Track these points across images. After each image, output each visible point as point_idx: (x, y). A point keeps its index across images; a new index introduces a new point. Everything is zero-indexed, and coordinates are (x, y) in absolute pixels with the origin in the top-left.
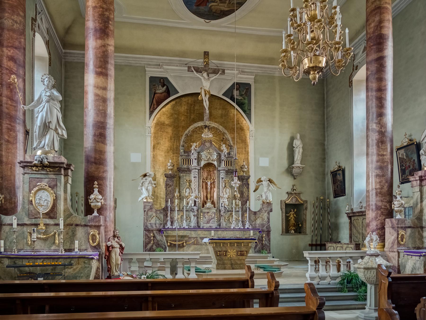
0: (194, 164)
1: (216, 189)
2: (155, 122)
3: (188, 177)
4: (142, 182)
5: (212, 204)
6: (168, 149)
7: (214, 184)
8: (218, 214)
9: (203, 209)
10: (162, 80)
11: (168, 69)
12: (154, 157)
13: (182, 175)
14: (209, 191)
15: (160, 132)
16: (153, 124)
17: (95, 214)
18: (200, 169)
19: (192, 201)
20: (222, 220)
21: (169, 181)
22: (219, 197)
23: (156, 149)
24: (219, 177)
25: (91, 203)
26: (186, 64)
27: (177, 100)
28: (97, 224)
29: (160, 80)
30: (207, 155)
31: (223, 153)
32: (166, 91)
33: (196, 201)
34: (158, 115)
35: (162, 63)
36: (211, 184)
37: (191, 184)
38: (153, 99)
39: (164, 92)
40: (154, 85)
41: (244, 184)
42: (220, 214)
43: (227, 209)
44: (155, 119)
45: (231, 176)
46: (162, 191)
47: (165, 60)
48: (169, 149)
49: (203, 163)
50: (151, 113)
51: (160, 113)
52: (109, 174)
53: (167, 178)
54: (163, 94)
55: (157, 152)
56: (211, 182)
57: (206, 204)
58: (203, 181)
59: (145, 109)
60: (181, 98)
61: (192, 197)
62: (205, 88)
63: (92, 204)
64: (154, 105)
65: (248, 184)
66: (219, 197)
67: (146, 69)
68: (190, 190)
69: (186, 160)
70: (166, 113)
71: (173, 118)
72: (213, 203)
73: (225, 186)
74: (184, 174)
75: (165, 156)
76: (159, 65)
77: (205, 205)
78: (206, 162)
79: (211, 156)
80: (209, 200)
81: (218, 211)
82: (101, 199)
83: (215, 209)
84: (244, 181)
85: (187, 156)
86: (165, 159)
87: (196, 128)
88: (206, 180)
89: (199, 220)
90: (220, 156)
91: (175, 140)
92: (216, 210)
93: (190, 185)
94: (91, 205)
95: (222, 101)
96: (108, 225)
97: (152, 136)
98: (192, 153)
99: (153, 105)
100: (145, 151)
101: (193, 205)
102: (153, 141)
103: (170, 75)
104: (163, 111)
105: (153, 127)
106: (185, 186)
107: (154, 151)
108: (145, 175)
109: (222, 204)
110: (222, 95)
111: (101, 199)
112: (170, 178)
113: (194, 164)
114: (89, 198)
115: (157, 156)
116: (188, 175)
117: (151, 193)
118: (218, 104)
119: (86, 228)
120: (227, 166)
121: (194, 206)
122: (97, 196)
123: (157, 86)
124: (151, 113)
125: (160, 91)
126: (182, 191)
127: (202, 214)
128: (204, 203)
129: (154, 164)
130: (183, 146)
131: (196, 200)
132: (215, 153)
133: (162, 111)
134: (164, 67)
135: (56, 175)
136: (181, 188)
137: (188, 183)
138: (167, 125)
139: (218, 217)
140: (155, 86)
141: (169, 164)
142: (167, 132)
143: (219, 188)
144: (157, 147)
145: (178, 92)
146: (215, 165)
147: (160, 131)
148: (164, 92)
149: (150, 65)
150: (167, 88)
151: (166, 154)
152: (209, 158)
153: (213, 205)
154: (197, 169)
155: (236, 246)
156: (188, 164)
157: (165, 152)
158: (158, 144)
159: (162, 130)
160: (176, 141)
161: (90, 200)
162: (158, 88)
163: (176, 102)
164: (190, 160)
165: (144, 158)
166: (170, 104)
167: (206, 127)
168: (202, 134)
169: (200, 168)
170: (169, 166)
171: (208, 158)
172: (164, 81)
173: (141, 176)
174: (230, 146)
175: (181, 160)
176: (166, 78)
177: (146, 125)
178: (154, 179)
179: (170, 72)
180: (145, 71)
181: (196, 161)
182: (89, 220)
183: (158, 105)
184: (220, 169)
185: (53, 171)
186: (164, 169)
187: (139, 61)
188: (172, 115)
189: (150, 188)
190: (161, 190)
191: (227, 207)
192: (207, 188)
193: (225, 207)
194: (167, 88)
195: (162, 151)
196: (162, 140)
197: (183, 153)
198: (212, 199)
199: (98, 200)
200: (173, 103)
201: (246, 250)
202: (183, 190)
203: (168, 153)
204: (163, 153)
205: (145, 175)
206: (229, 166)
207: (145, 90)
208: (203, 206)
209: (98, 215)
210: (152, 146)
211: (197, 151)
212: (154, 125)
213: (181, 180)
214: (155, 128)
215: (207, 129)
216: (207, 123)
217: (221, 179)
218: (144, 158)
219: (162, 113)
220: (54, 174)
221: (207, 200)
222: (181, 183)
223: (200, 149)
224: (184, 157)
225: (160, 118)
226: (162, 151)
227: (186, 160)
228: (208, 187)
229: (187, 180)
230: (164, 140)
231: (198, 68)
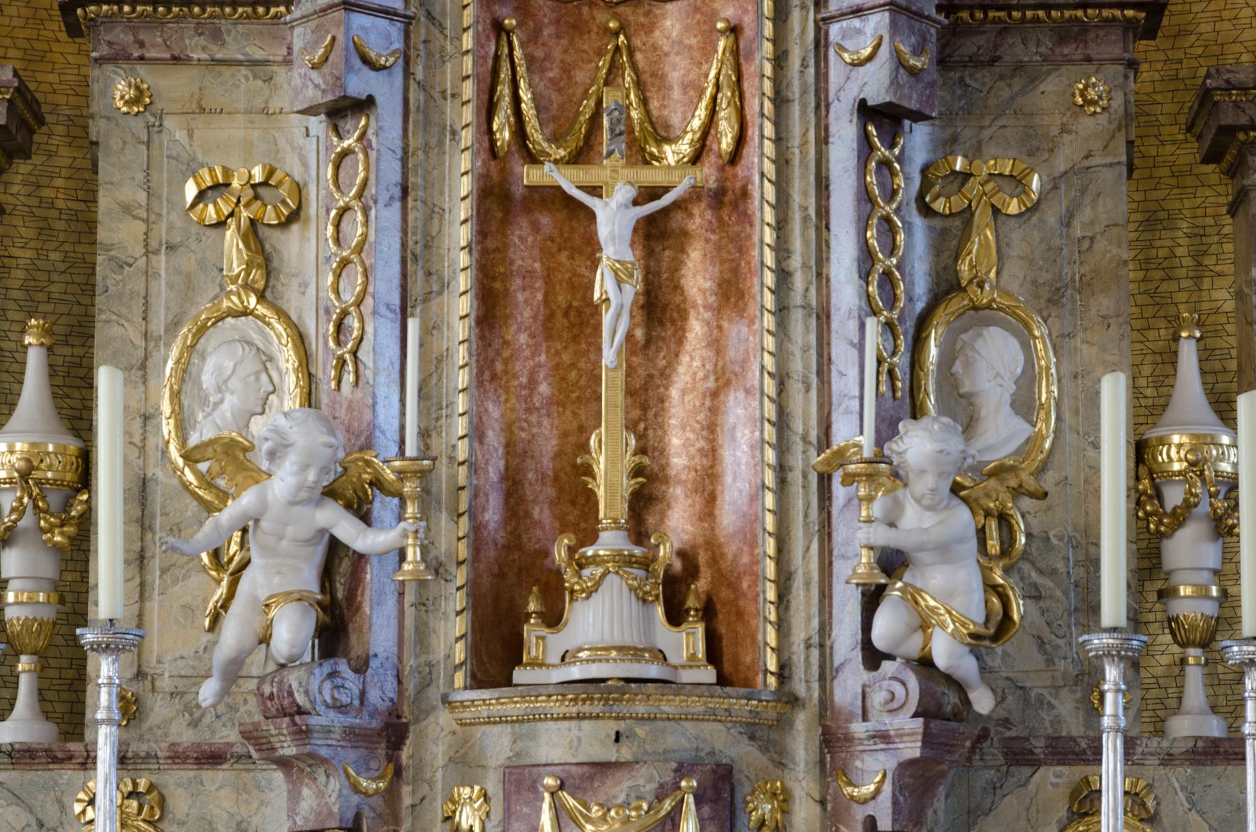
3: (234, 130)
5: (675, 617)
9: (487, 700)
33: (360, 559)
43: (983, 702)
56: (649, 194)
57: (553, 619)
68: (266, 360)
77: (532, 631)
80: (610, 541)
83: (736, 703)
116: (244, 85)
131: (348, 530)
137: (231, 238)
191: (967, 667)
193: (925, 663)
221: (591, 537)
228: (604, 284)
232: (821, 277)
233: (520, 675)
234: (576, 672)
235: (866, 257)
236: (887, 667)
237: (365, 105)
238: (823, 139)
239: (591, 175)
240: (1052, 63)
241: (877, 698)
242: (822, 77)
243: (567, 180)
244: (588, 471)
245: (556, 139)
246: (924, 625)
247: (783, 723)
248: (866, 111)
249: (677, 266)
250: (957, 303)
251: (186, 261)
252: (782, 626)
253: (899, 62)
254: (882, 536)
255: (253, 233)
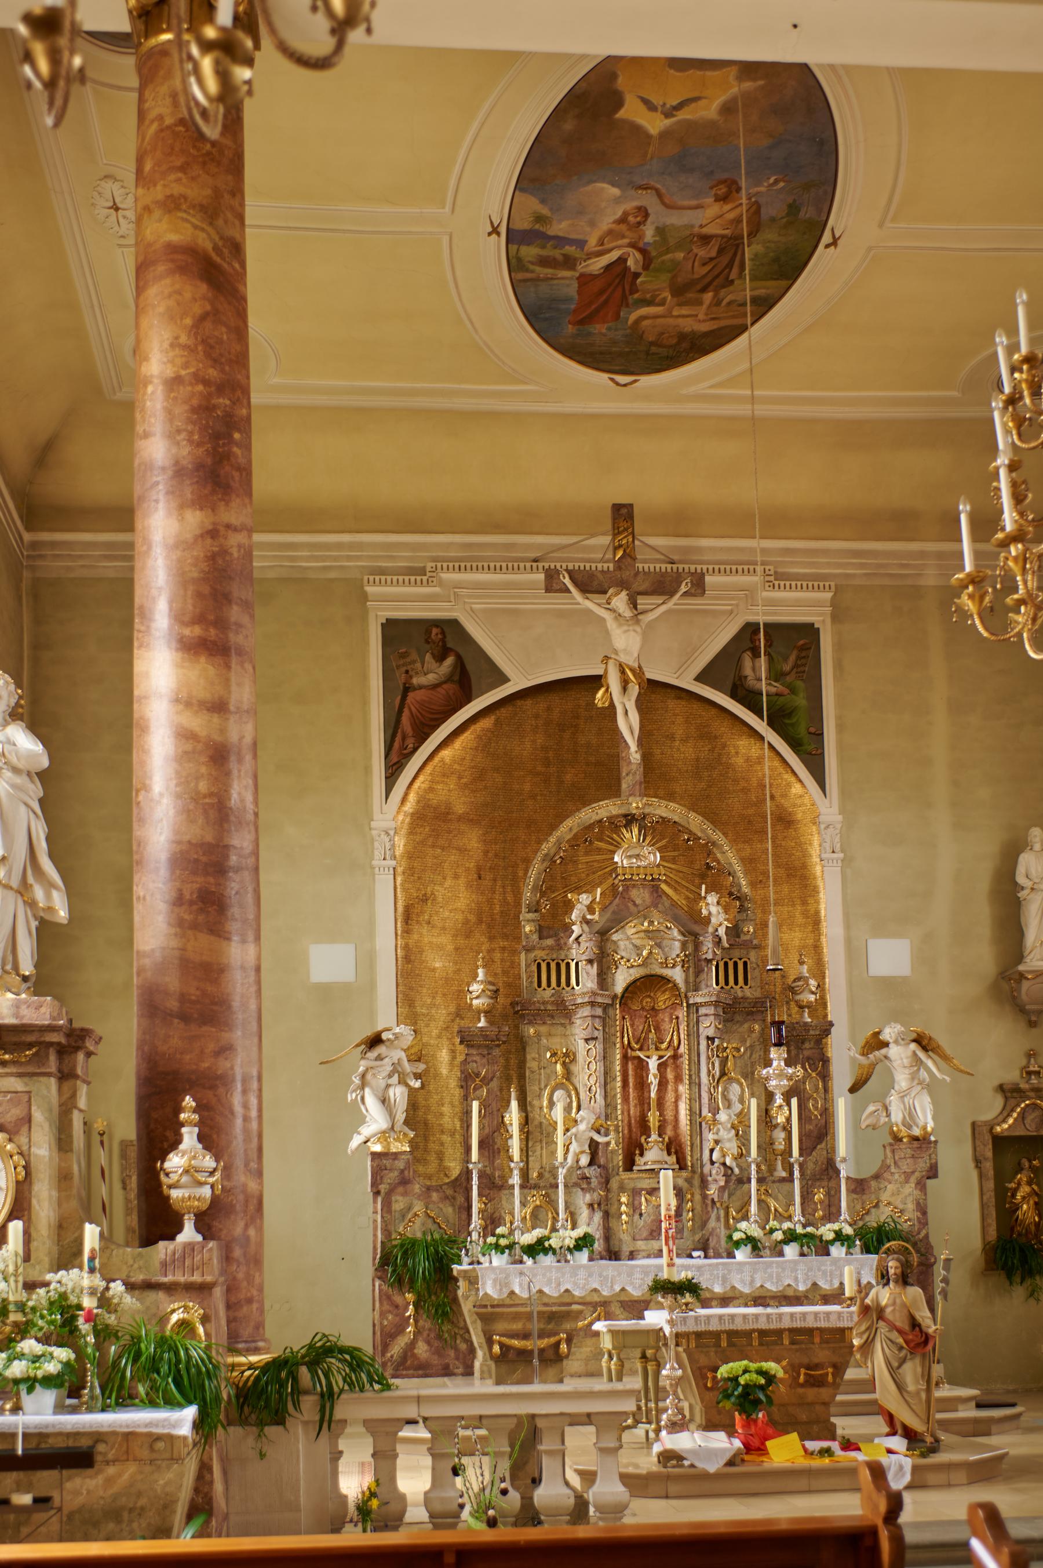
0: (586, 981)
1: (683, 1089)
2: (409, 807)
4: (361, 1069)
5: (669, 1154)
6: (466, 922)
7: (677, 1068)
8: (698, 1197)
10: (435, 631)
11: (459, 585)
12: (407, 959)
13: (532, 1031)
14: (653, 1095)
15: (430, 851)
16: (401, 817)
17: (188, 1234)
18: (612, 1005)
19: (581, 1145)
20: (712, 1223)
21: (477, 1058)
22: (697, 1125)
23: (418, 922)
24: (693, 1034)
25: (170, 1187)
26: (535, 560)
27: (503, 712)
28: (197, 1278)
29: (428, 632)
30: (638, 942)
31: (711, 929)
32: (456, 678)
33: (597, 1143)
34: (421, 778)
35: (435, 560)
36: (661, 1067)
37: (575, 1069)
38: (400, 712)
39: (445, 682)
40: (403, 656)
41: (808, 1059)
42: (704, 1197)
43: (737, 1171)
44: (412, 797)
45: (746, 1026)
46: (447, 1100)
47: (448, 546)
48: (472, 918)
49: (621, 980)
50: (393, 772)
51: (429, 769)
52: (239, 1061)
53: (468, 1046)
54: (439, 689)
55: (421, 934)
56: (661, 1057)
57: (642, 1155)
58: (625, 1058)
59: (369, 757)
60: (519, 703)
61: (582, 1127)
62: (623, 658)
63: (175, 1194)
64: (404, 739)
65: (826, 1061)
66: (697, 1125)
67: (369, 589)
68: (570, 1096)
69: (548, 965)
70: (456, 766)
71: (486, 787)
72: (673, 1147)
73: (723, 1074)
74: (543, 1029)
75: (457, 949)
76: (422, 571)
77: (637, 1158)
78: (636, 973)
79: (659, 945)
80: (654, 1137)
81: (696, 1182)
82: (212, 1173)
84: (807, 1045)
85: (551, 948)
86: (455, 963)
87: (590, 827)
88: (640, 1049)
89: (613, 1223)
90: (697, 946)
91: (495, 880)
92: (688, 1181)
93: (568, 1075)
94: (168, 1198)
95: (696, 705)
96: (240, 1276)
97: (400, 870)
98: (574, 936)
99: (398, 739)
100: (371, 934)
101: (584, 1160)
102: (405, 890)
103: (467, 607)
104: (442, 760)
105: (404, 832)
106: (548, 1079)
107: (407, 931)
108: (375, 1041)
109: (712, 1151)
110: (695, 679)
111: (212, 1173)
112: (479, 1047)
113: (586, 981)
114: (162, 1168)
115: (421, 952)
116: (560, 1029)
117: (401, 1117)
118: (680, 720)
119: (152, 1296)
120: (727, 983)
121: (590, 1164)
122: (194, 1158)
123: (414, 655)
124: (393, 772)
125: (431, 678)
126: (536, 1103)
127: (624, 1199)
128: (633, 1150)
129: (411, 989)
130: (535, 909)
132: (675, 933)
133: (436, 759)
134: (444, 576)
135: (26, 1079)
136: (531, 1089)
137: (559, 1067)
138: (460, 818)
139: (698, 1207)
140: (408, 660)
141: (476, 988)
142: (462, 850)
143: (695, 1083)
144: (422, 912)
145: (504, 679)
146: (675, 985)
147: (433, 846)
148: (445, 682)
149: (382, 571)
150: (460, 663)
151: (461, 941)
152: (651, 953)
153: (673, 1158)
154: (600, 1005)
155: (786, 1342)
156: (559, 984)
157: (455, 936)
158: (424, 899)
159: (441, 842)
160: (499, 883)
161: (167, 1175)
162: (418, 665)
163: (497, 720)
164: (568, 965)
165: (367, 962)
166: (472, 728)
167: (630, 819)
168: (614, 852)
169: (609, 1001)
170: (475, 994)
171: (645, 953)
172: (445, 637)
173: (357, 1046)
174: (738, 898)
175: (528, 966)
176: (454, 624)
177: (373, 824)
178: (416, 1058)
179: (470, 597)
180: (364, 597)
181: (594, 970)
182: (164, 1265)
183: (422, 738)
184: (699, 1000)
185: (13, 1062)
186: (452, 1009)
187: (336, 559)
188: (480, 775)
189: (398, 1094)
190: (442, 1099)
191: (734, 1165)
192: (642, 1085)
193: (724, 1164)
194: (459, 658)
195: (444, 928)
196: (442, 884)
197: (535, 937)
198: (669, 1132)
199: (202, 1177)
200: (486, 723)
201: (835, 1359)
202: (540, 1096)
203: (468, 936)
204: (445, 940)
205: (375, 1041)
206: (736, 983)
207: (364, 677)
208: (629, 1164)
209: (199, 1238)
210: (400, 909)
211: (597, 927)
212: (408, 820)
213: (531, 1054)
214: (412, 832)
215: (635, 831)
216: (636, 805)
217: (703, 1043)
218: (367, 962)
219: (438, 769)
220: (20, 1075)
221: (649, 1136)
222: (531, 1064)
223: (608, 915)
224: (539, 954)
225: (431, 789)
226: (444, 928)
227: (548, 965)
228: (651, 1078)
229: (554, 1055)
230: (449, 882)
231: (591, 575)
232: (699, 1077)
233: (635, 1168)
234: (648, 1167)
235: (709, 1071)
236: (716, 1165)
237: (595, 1039)
238: (699, 1044)
239: (648, 1053)
240: (745, 1021)
241: (714, 1172)
242: (698, 1029)
243: (641, 1055)
244: (648, 1121)
245: (637, 1043)
246: (724, 1156)
247: (692, 1177)
248: (708, 1038)
249: (666, 1072)
250: (726, 1078)
251: (548, 1071)
252: (692, 1156)
253: (716, 1027)
254: (716, 1137)
255: (564, 1064)
